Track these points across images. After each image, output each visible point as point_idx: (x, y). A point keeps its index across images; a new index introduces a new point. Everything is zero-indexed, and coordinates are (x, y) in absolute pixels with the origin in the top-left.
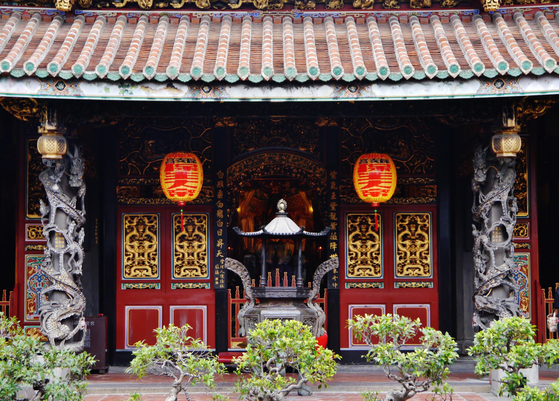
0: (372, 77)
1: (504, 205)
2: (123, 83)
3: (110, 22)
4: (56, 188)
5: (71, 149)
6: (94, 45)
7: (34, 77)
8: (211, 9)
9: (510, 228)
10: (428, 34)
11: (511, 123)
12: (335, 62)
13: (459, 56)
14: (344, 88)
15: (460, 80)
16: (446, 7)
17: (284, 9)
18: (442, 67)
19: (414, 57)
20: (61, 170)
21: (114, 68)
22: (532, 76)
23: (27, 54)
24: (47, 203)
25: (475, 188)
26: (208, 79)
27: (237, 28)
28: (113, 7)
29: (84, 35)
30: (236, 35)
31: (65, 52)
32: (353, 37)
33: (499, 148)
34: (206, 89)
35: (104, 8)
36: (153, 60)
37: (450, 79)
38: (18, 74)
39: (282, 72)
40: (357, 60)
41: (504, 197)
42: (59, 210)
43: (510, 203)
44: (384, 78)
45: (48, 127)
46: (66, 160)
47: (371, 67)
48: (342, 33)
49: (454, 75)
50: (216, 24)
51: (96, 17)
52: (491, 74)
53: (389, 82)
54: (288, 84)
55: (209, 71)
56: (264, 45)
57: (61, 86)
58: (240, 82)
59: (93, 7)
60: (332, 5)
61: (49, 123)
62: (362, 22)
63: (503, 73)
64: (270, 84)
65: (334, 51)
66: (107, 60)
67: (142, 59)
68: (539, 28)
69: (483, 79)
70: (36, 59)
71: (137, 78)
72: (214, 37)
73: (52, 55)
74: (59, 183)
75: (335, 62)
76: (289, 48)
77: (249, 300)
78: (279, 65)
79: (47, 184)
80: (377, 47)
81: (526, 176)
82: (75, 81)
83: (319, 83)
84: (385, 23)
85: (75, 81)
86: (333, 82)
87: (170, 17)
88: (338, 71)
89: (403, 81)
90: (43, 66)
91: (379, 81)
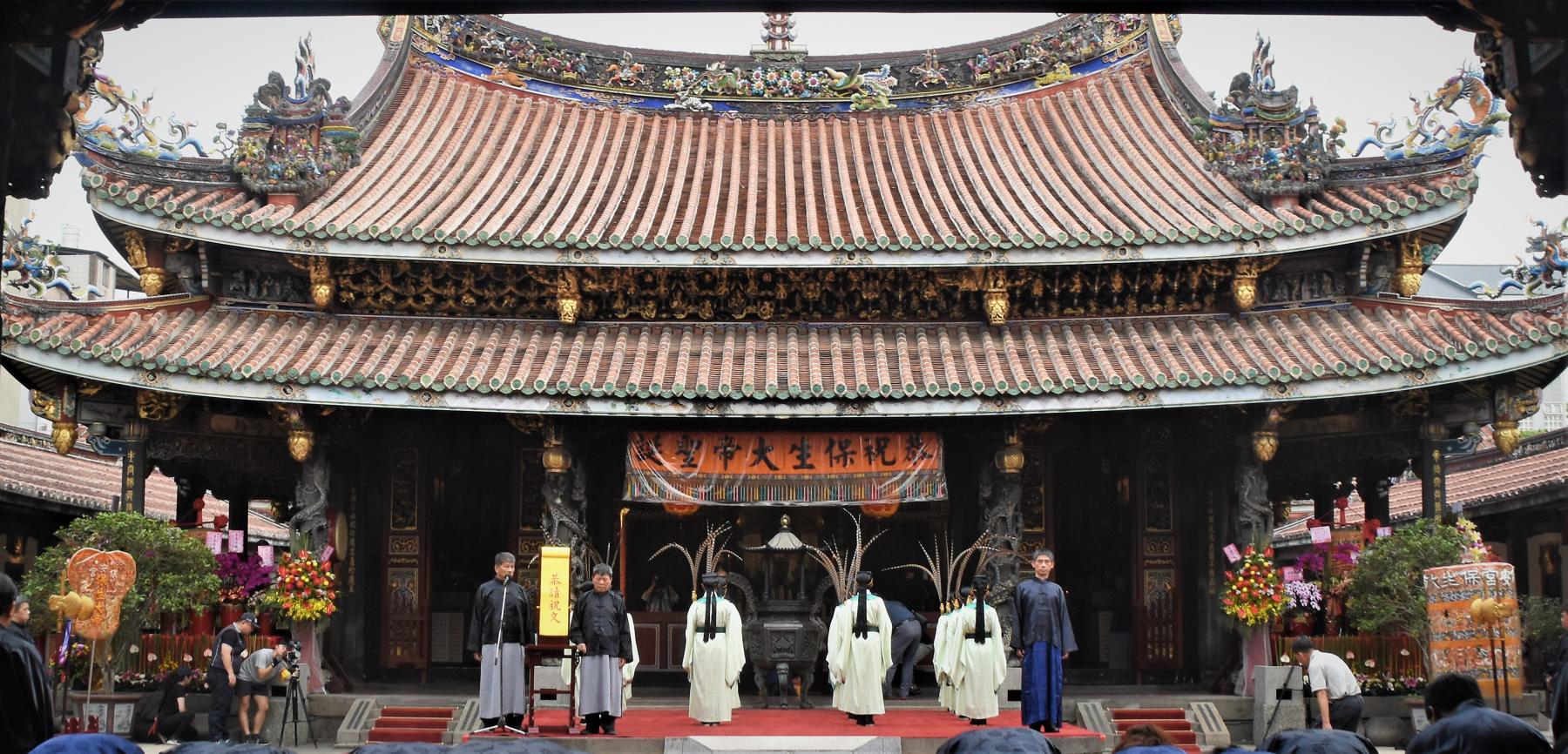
0: (874, 395)
1: (1009, 521)
2: (631, 399)
3: (613, 335)
4: (559, 501)
5: (574, 464)
6: (598, 359)
7: (544, 395)
8: (715, 319)
9: (1015, 545)
10: (934, 347)
11: (1013, 440)
12: (839, 379)
13: (963, 372)
14: (847, 406)
15: (961, 398)
16: (954, 319)
17: (789, 319)
18: (944, 385)
19: (918, 374)
20: (563, 483)
21: (621, 384)
22: (1030, 395)
23: (536, 371)
24: (549, 516)
25: (981, 503)
26: (713, 396)
27: (740, 340)
28: (616, 319)
29: (589, 348)
30: (740, 348)
31: (571, 368)
32: (858, 351)
33: (1002, 463)
34: (711, 405)
35: (607, 319)
36: (659, 377)
37: (950, 398)
38: (528, 392)
39: (787, 388)
40: (862, 378)
41: (1010, 513)
42: (561, 523)
43: (1015, 519)
44: (887, 395)
45: (554, 442)
46: (569, 475)
47: (874, 382)
48: (847, 346)
49: (955, 394)
50: (719, 336)
51: (598, 329)
52: (991, 393)
53: (891, 400)
54: (793, 401)
55: (714, 388)
56: (769, 359)
57: (569, 403)
58: (744, 399)
59: (596, 318)
60: (838, 315)
61: (556, 439)
62: (868, 335)
63: (1002, 392)
64: (773, 401)
65: (838, 364)
66: (613, 377)
67: (648, 374)
68: (1045, 343)
69: (983, 398)
70: (545, 376)
71: (643, 395)
72: (718, 350)
73: (559, 371)
74: (561, 497)
75: (839, 379)
76: (793, 360)
77: (752, 614)
78: (783, 381)
79: (549, 498)
80: (882, 360)
81: (1042, 490)
82: (582, 398)
83: (822, 400)
84: (891, 336)
85: (582, 398)
87: (673, 327)
88: (841, 388)
89: (905, 399)
90: (552, 384)
91: (881, 399)
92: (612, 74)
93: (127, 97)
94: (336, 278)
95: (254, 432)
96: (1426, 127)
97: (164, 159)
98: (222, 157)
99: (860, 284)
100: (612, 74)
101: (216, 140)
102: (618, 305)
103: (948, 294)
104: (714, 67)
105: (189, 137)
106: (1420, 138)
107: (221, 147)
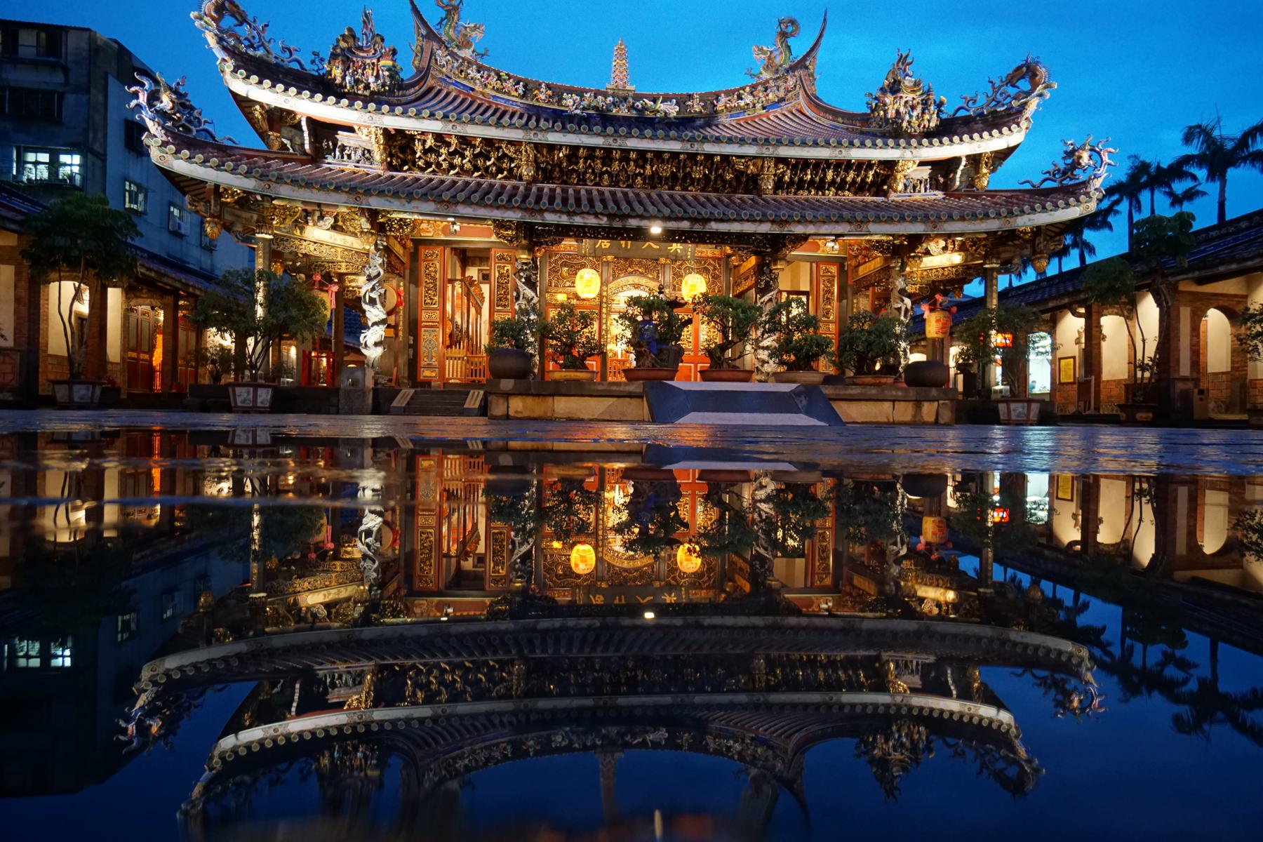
59: (543, 182)
86: (690, 219)
92: (536, 95)
93: (250, 18)
94: (390, 146)
95: (342, 243)
96: (998, 96)
97: (277, 65)
98: (316, 74)
99: (692, 168)
100: (536, 95)
101: (313, 62)
102: (556, 174)
103: (739, 174)
104: (588, 95)
105: (294, 57)
106: (994, 103)
107: (316, 68)
